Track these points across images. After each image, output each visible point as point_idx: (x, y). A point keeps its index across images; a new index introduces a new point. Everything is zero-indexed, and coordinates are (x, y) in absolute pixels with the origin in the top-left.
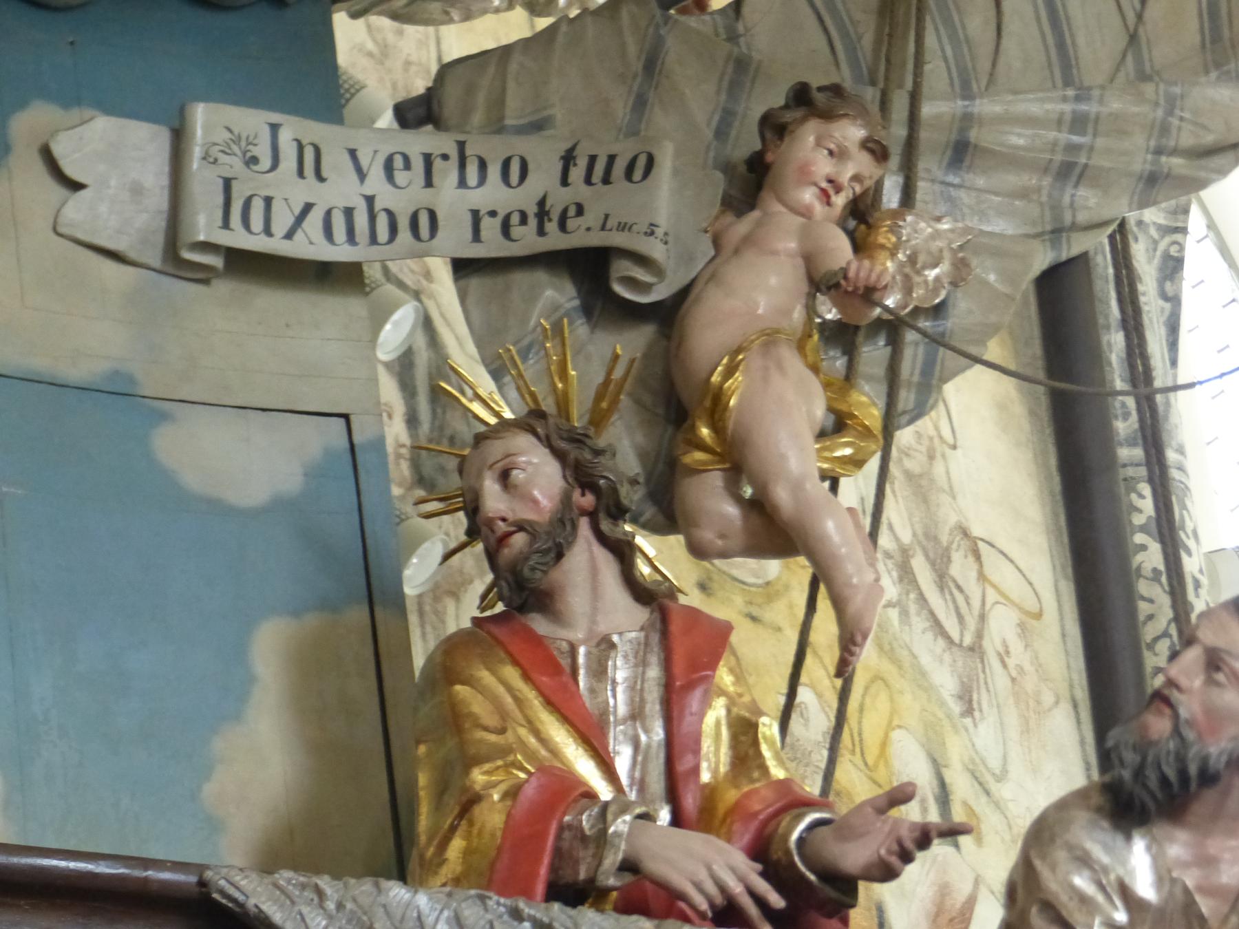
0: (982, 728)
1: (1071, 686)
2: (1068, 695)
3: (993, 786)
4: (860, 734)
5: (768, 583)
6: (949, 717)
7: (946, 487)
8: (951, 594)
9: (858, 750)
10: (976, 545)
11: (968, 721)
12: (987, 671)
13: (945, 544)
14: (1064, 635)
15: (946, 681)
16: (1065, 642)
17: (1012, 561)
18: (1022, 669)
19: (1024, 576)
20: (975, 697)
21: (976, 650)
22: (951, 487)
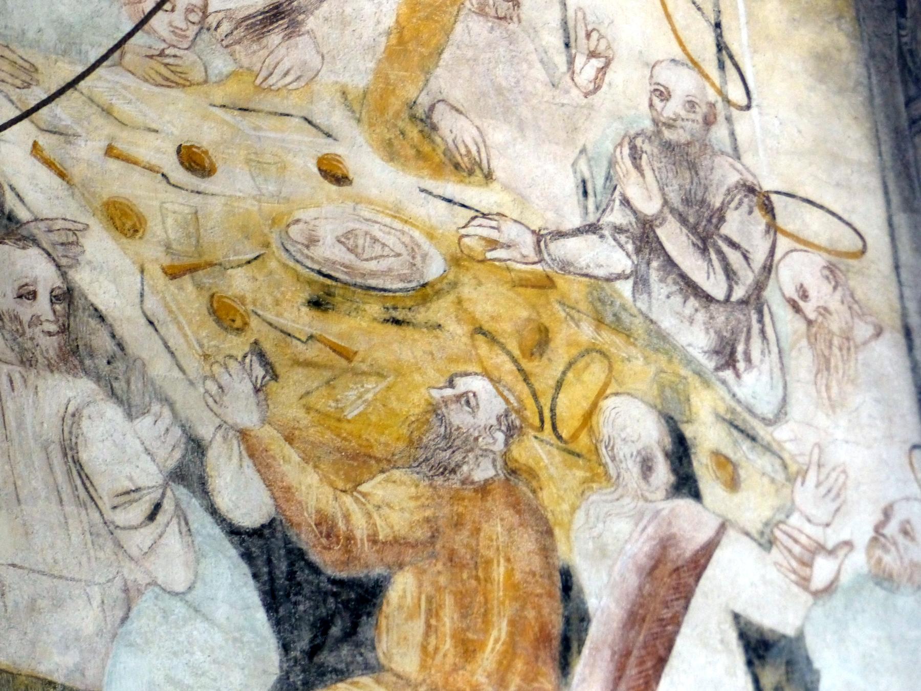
0: (748, 378)
1: (904, 315)
2: (898, 323)
3: (761, 431)
5: (424, 286)
7: (729, 149)
8: (719, 252)
9: (548, 425)
10: (768, 198)
11: (728, 374)
12: (767, 319)
13: (718, 205)
14: (897, 267)
15: (695, 338)
16: (898, 275)
17: (821, 207)
18: (826, 309)
19: (840, 218)
20: (740, 348)
21: (755, 300)
22: (736, 149)
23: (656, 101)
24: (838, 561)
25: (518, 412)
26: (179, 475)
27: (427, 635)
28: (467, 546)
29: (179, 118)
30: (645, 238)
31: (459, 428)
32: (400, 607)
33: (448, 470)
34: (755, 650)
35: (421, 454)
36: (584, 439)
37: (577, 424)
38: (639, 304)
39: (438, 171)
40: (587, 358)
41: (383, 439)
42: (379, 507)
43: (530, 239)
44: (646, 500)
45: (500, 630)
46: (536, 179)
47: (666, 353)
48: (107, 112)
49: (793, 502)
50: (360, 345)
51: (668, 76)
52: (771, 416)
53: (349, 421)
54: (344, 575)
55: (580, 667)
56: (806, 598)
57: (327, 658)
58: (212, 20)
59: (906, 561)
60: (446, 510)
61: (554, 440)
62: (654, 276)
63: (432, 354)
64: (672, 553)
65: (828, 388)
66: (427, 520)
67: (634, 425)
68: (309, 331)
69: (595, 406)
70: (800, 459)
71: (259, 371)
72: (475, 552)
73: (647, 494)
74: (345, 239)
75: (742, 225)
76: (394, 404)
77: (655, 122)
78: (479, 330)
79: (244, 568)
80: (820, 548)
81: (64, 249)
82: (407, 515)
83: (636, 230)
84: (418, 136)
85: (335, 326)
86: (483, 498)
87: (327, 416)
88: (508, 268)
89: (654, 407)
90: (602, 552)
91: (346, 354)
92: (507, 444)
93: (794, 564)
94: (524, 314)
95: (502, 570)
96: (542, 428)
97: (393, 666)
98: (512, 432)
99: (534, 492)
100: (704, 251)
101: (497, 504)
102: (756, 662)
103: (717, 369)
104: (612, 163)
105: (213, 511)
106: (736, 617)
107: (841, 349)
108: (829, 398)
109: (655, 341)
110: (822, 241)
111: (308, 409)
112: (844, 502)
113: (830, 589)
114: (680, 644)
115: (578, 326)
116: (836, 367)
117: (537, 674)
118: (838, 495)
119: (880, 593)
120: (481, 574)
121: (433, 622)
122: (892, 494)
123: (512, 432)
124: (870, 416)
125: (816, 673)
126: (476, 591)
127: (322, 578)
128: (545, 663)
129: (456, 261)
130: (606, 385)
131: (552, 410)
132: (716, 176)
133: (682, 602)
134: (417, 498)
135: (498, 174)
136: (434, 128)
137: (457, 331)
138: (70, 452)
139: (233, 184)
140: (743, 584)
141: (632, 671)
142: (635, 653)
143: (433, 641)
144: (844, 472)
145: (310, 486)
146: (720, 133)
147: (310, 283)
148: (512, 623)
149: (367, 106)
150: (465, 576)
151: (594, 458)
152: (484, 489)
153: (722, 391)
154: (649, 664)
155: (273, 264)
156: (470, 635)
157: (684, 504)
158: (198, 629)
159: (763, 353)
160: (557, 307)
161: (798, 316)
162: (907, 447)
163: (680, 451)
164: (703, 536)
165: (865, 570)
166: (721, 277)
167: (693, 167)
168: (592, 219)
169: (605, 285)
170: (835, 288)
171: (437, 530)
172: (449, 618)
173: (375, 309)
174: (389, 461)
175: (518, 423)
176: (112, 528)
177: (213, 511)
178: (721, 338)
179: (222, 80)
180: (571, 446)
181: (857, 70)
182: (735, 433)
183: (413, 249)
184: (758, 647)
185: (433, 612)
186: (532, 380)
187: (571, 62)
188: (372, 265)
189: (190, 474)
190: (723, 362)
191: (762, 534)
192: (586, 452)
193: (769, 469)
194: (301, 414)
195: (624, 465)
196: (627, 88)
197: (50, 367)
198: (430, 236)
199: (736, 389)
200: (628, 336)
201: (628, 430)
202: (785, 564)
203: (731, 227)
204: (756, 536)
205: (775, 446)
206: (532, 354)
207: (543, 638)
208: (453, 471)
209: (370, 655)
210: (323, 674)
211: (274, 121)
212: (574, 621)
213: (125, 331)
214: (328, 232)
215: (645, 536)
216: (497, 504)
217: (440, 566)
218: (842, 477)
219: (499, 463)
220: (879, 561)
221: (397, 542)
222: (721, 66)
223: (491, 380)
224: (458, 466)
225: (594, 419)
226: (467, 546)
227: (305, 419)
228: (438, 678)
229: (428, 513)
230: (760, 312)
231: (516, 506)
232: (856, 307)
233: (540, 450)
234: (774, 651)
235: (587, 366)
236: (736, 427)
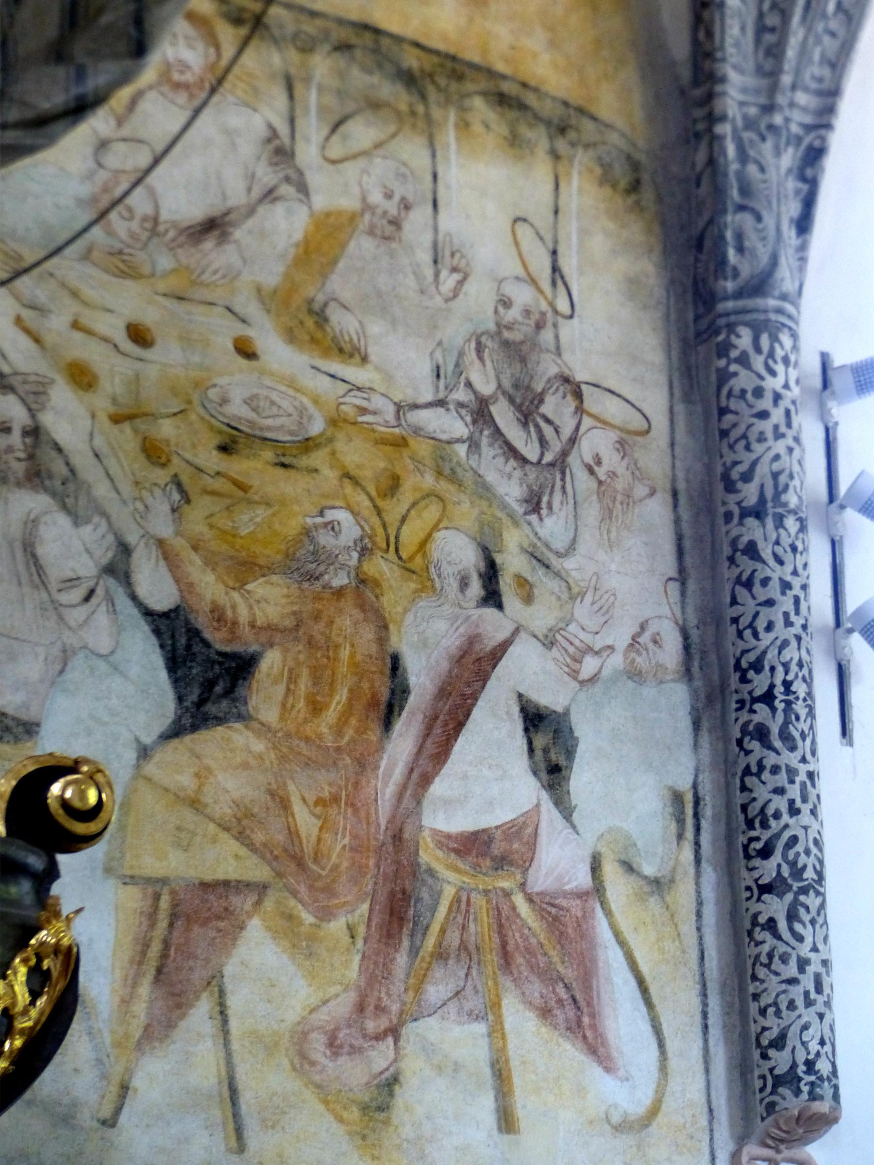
0: (549, 522)
1: (674, 480)
2: (668, 487)
3: (554, 561)
4: (397, 538)
5: (307, 439)
6: (511, 516)
7: (552, 348)
8: (537, 426)
10: (579, 387)
11: (534, 518)
13: (540, 390)
14: (672, 445)
15: (511, 489)
16: (673, 450)
17: (619, 396)
18: (614, 473)
19: (633, 405)
20: (545, 499)
21: (560, 464)
22: (558, 348)
23: (501, 309)
24: (601, 660)
25: (370, 537)
26: (110, 570)
27: (286, 696)
28: (323, 634)
29: (130, 302)
30: (481, 413)
31: (324, 547)
32: (268, 675)
33: (313, 577)
34: (532, 720)
35: (294, 565)
36: (418, 560)
37: (414, 548)
38: (471, 462)
39: (326, 353)
40: (427, 501)
41: (266, 552)
42: (259, 602)
43: (392, 409)
44: (461, 607)
45: (342, 695)
46: (401, 363)
47: (488, 499)
48: (75, 294)
49: (572, 614)
50: (255, 482)
51: (512, 290)
52: (562, 551)
53: (241, 538)
54: (228, 649)
55: (399, 726)
56: (575, 685)
57: (211, 708)
58: (161, 228)
59: (653, 662)
60: (309, 607)
61: (396, 560)
62: (485, 441)
63: (309, 491)
64: (477, 647)
65: (609, 532)
66: (294, 613)
67: (457, 551)
68: (217, 468)
69: (429, 535)
70: (582, 584)
71: (176, 496)
72: (328, 638)
73: (462, 603)
74: (250, 401)
75: (556, 407)
76: (277, 527)
77: (498, 324)
78: (347, 475)
79: (154, 640)
80: (590, 650)
81: (35, 396)
82: (279, 608)
83: (474, 406)
84: (313, 326)
85: (237, 466)
86: (338, 600)
87: (224, 532)
88: (373, 431)
89: (475, 539)
90: (424, 643)
91: (243, 487)
92: (360, 561)
93: (568, 660)
94: (382, 465)
95: (347, 652)
96: (387, 550)
97: (260, 717)
98: (364, 552)
99: (377, 597)
100: (525, 424)
101: (348, 605)
102: (532, 729)
103: (526, 513)
104: (461, 354)
105: (134, 597)
106: (520, 696)
107: (622, 504)
108: (609, 539)
109: (480, 490)
110: (617, 422)
111: (211, 526)
112: (612, 617)
113: (593, 679)
114: (476, 713)
115: (422, 476)
116: (617, 517)
117: (366, 729)
118: (607, 612)
119: (631, 684)
120: (331, 654)
121: (292, 687)
122: (648, 613)
123: (364, 552)
124: (639, 555)
125: (577, 739)
126: (326, 666)
127: (211, 651)
128: (373, 720)
129: (335, 422)
130: (440, 521)
131: (397, 538)
132: (541, 368)
133: (481, 683)
134: (288, 596)
135: (372, 357)
136: (326, 320)
137: (329, 474)
138: (29, 548)
139: (168, 356)
140: (529, 672)
141: (437, 730)
142: (441, 718)
143: (290, 700)
144: (614, 595)
145: (207, 583)
146: (547, 336)
147: (220, 432)
148: (351, 691)
149: (276, 300)
150: (319, 655)
151: (425, 574)
152: (339, 593)
153: (527, 530)
154: (451, 726)
155: (193, 417)
156: (319, 698)
157: (490, 612)
158: (116, 683)
159: (562, 503)
160: (408, 461)
161: (592, 477)
162: (666, 578)
163: (491, 573)
164: (501, 636)
165: (622, 667)
166: (536, 444)
167: (523, 360)
168: (441, 395)
169: (446, 446)
170: (623, 458)
171: (301, 621)
172: (304, 684)
173: (268, 455)
174: (269, 568)
175: (369, 546)
176: (57, 606)
177: (134, 597)
178: (532, 491)
179: (166, 274)
180: (409, 565)
181: (659, 293)
182: (534, 562)
183: (302, 411)
184: (534, 718)
185: (293, 679)
186: (384, 515)
187: (437, 275)
188: (269, 422)
189: (119, 569)
190: (530, 508)
191: (546, 636)
192: (419, 571)
193: (556, 590)
194: (205, 529)
195: (446, 581)
196: (479, 297)
197: (19, 484)
198: (316, 402)
199: (538, 530)
200: (460, 486)
201: (453, 555)
202: (561, 659)
203: (548, 408)
204: (542, 638)
205: (563, 574)
206: (385, 495)
207: (373, 703)
208: (317, 579)
209: (242, 708)
210: (206, 720)
211: (202, 309)
212: (398, 692)
213: (77, 461)
214: (237, 396)
215: (457, 634)
216: (348, 605)
217: (300, 647)
218: (612, 598)
219: (353, 574)
220: (633, 661)
221: (270, 627)
222: (554, 284)
223: (352, 512)
224: (321, 575)
225: (428, 545)
226: (323, 634)
227: (208, 534)
228: (291, 726)
229: (295, 608)
230: (563, 473)
231: (362, 606)
232: (637, 473)
233: (384, 566)
234: (546, 722)
235: (427, 507)
236: (535, 558)
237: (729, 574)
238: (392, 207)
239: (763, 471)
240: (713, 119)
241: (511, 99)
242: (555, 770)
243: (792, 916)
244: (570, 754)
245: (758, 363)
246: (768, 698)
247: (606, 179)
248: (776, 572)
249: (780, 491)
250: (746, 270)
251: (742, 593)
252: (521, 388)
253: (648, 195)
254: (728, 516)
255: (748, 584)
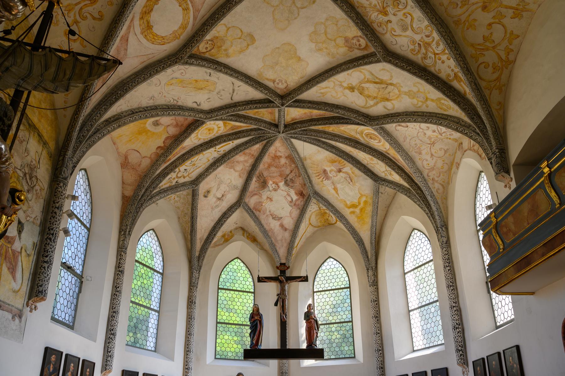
237: (50, 215)
238: (22, 139)
239: (60, 203)
240: (65, 155)
241: (40, 136)
242: (20, 231)
243: (48, 267)
244: (23, 230)
245: (63, 188)
246: (53, 234)
247: (48, 154)
248: (58, 218)
249: (61, 207)
250: (64, 176)
251: (52, 218)
252: (30, 174)
253: (52, 159)
254: (53, 207)
255: (54, 217)
